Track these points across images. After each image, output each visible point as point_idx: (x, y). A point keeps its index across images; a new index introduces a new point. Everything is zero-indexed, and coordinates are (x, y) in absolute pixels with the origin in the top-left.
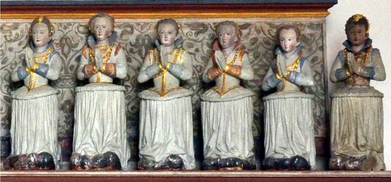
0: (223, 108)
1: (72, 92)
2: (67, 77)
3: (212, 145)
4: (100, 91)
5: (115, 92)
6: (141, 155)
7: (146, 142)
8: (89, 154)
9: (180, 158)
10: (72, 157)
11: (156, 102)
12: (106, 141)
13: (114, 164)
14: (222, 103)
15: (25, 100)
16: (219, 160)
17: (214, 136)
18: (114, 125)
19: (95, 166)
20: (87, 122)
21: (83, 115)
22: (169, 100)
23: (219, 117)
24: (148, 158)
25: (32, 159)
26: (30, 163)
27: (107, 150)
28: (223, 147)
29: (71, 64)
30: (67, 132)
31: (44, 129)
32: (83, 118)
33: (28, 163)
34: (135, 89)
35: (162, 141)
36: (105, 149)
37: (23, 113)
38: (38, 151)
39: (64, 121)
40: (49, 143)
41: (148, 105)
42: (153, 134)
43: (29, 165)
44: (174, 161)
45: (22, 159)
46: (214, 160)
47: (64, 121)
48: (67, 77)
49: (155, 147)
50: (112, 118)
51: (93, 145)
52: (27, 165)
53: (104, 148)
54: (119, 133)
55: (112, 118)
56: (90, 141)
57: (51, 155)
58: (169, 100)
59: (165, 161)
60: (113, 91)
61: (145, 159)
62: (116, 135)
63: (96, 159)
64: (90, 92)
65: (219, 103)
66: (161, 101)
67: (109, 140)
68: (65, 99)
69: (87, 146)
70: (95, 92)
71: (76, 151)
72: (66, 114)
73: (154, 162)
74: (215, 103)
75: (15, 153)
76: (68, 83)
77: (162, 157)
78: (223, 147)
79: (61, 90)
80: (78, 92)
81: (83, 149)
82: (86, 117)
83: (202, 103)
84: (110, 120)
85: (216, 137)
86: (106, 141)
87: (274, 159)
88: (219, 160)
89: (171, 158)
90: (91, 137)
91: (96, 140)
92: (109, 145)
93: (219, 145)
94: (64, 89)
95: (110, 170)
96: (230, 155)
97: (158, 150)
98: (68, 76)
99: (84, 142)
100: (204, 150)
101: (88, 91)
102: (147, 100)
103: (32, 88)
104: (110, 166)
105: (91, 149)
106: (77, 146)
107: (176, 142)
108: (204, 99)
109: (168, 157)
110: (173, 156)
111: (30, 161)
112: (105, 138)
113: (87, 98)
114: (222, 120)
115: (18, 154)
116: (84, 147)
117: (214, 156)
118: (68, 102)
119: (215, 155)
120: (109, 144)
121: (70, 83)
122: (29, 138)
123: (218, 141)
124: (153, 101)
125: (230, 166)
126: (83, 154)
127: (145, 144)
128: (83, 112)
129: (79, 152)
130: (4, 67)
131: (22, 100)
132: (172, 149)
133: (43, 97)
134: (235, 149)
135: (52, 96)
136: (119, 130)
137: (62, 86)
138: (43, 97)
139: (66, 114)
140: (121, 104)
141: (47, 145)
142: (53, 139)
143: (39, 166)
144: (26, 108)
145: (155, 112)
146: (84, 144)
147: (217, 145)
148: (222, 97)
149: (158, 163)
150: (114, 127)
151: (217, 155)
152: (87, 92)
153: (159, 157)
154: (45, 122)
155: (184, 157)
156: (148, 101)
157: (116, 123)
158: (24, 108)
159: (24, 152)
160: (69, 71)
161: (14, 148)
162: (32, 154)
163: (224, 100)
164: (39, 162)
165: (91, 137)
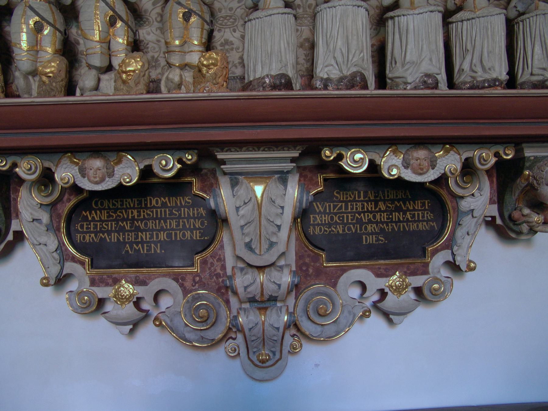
0: (478, 25)
1: (310, 30)
2: (305, 16)
3: (466, 66)
4: (343, 5)
5: (360, 8)
6: (389, 79)
7: (396, 63)
8: (332, 76)
9: (435, 77)
10: (314, 79)
11: (406, 17)
12: (352, 60)
13: (362, 83)
14: (477, 19)
15: (258, 18)
16: (475, 82)
17: (468, 58)
18: (360, 43)
19: (340, 87)
20: (329, 42)
21: (324, 34)
22: (422, 13)
23: (474, 36)
24: (397, 80)
25: (267, 81)
26: (264, 85)
27: (354, 69)
28: (479, 69)
29: (308, 3)
30: (307, 69)
31: (281, 49)
32: (325, 38)
33: (262, 85)
34: (374, 27)
35: (414, 59)
36: (351, 69)
37: (256, 33)
38: (273, 73)
39: (304, 59)
40: (286, 65)
41: (396, 23)
42: (403, 53)
43: (264, 88)
44: (430, 81)
45: (255, 83)
46: (470, 82)
47: (304, 59)
48: (305, 16)
49: (406, 67)
50: (358, 36)
51: (337, 67)
52: (262, 88)
53: (349, 69)
54: (365, 54)
55: (358, 36)
56: (333, 62)
57: (288, 76)
58: (422, 13)
59: (419, 81)
60: (358, 7)
61: (395, 82)
62: (362, 55)
63: (341, 79)
64: (331, 9)
65: (474, 20)
66: (412, 14)
67: (355, 60)
68: (304, 37)
69: (331, 68)
70: (337, 7)
71: (317, 75)
72: (305, 52)
73: (406, 83)
74: (468, 22)
75: (248, 78)
76: (306, 21)
77: (416, 77)
78: (479, 69)
79: (299, 28)
80: (318, 12)
81: (326, 72)
82: (328, 37)
83: (450, 26)
84: (355, 37)
85: (471, 58)
86: (352, 60)
87: (532, 82)
88: (475, 82)
89: (426, 77)
90: (334, 58)
91: (340, 59)
92: (355, 65)
93: (475, 65)
94: (303, 28)
95: (356, 90)
96: (487, 76)
97: (411, 69)
98: (306, 14)
99: (326, 64)
100: (455, 75)
101: (329, 8)
102: (395, 16)
103: (267, 7)
104: (357, 86)
105: (335, 72)
106: (318, 70)
107: (431, 60)
108: (454, 21)
109: (422, 76)
110: (428, 76)
111: (265, 82)
112: (350, 58)
113: (328, 15)
114: (478, 38)
115: (251, 79)
116: (326, 69)
117: (469, 79)
118: (307, 40)
119: (470, 78)
120: (355, 63)
121: (309, 21)
122: (264, 59)
123: (474, 61)
124: (402, 17)
125: (490, 87)
126: (326, 76)
127: (394, 65)
128: (325, 31)
129: (321, 75)
130: (240, 7)
131: (254, 19)
132: (425, 67)
133: (278, 14)
134: (492, 69)
135: (290, 16)
136: (365, 51)
137: (301, 24)
138: (278, 14)
139: (305, 52)
140: (366, 22)
141: (285, 67)
142: (291, 62)
143: (274, 87)
144: (260, 27)
145: (405, 28)
146: (326, 66)
147: (473, 65)
148: (477, 13)
149: (410, 83)
150: (360, 46)
151: (471, 77)
152: (328, 9)
153: (413, 76)
154: (282, 42)
155: (439, 77)
156: (396, 19)
157: (362, 43)
158: (257, 28)
159: (257, 77)
160: (308, 9)
161: (248, 75)
162: (267, 76)
163: (480, 15)
164: (274, 84)
165: (334, 58)
